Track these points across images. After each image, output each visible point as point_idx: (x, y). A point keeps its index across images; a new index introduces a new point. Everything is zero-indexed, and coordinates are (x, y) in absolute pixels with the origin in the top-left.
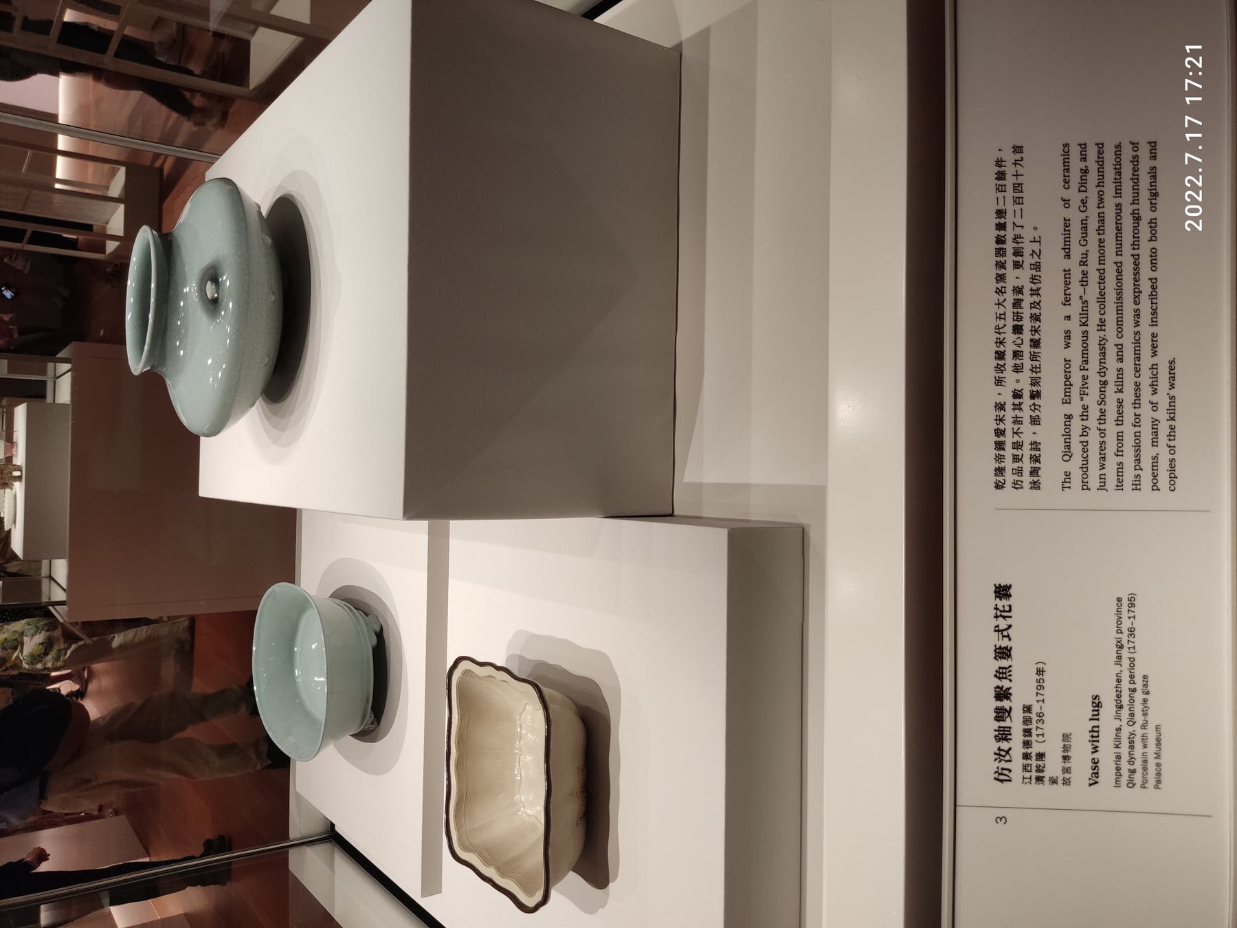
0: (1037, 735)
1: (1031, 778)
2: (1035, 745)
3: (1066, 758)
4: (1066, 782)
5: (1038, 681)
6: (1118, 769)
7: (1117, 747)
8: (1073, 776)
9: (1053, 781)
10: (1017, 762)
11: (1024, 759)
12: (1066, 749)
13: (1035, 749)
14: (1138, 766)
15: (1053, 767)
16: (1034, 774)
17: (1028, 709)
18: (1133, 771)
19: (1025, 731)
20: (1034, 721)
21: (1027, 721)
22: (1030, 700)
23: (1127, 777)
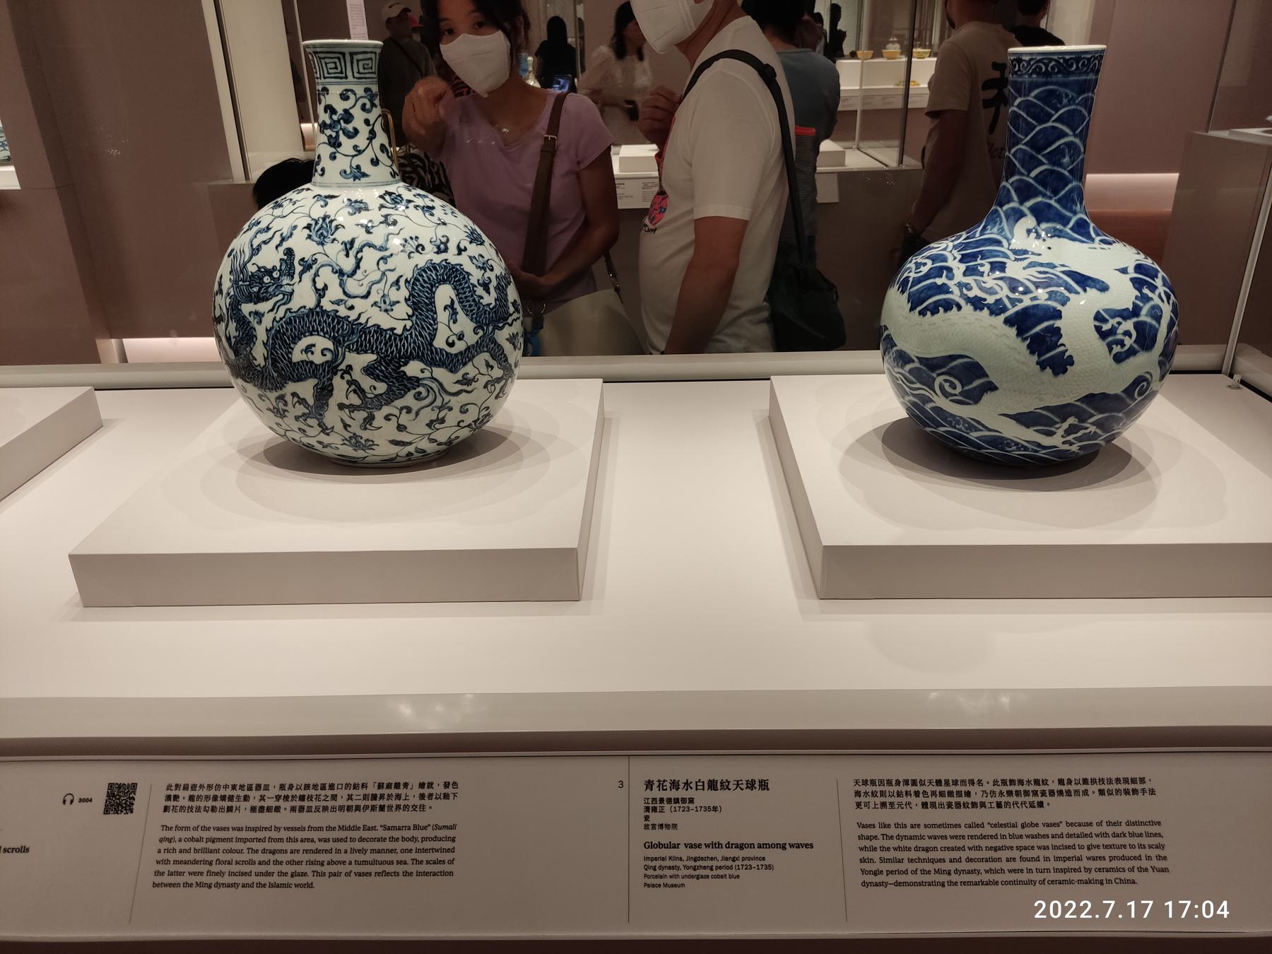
0: (675, 807)
1: (648, 803)
2: (669, 806)
3: (661, 826)
4: (646, 827)
5: (709, 807)
6: (656, 859)
7: (670, 858)
8: (650, 831)
9: (647, 818)
10: (656, 793)
11: (660, 798)
12: (668, 826)
13: (667, 806)
14: (659, 872)
15: (655, 818)
16: (651, 805)
17: (691, 801)
18: (655, 870)
19: (678, 799)
20: (684, 805)
21: (684, 800)
22: (697, 803)
23: (651, 865)
